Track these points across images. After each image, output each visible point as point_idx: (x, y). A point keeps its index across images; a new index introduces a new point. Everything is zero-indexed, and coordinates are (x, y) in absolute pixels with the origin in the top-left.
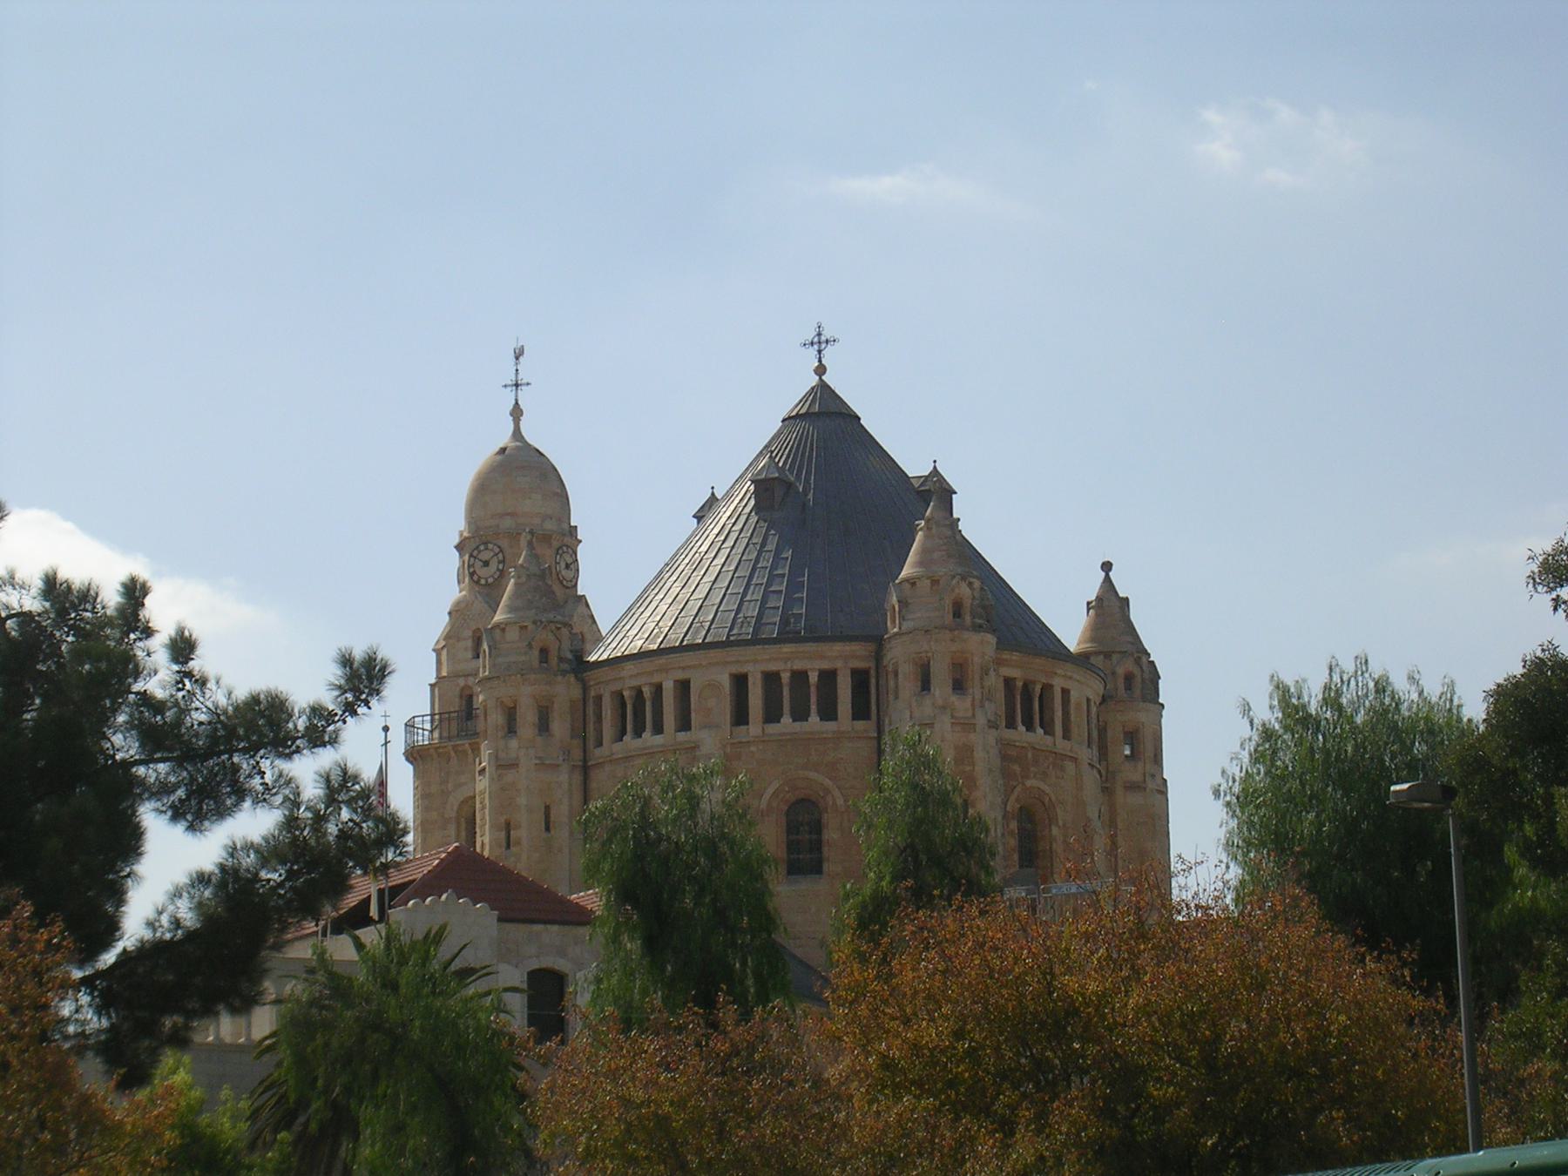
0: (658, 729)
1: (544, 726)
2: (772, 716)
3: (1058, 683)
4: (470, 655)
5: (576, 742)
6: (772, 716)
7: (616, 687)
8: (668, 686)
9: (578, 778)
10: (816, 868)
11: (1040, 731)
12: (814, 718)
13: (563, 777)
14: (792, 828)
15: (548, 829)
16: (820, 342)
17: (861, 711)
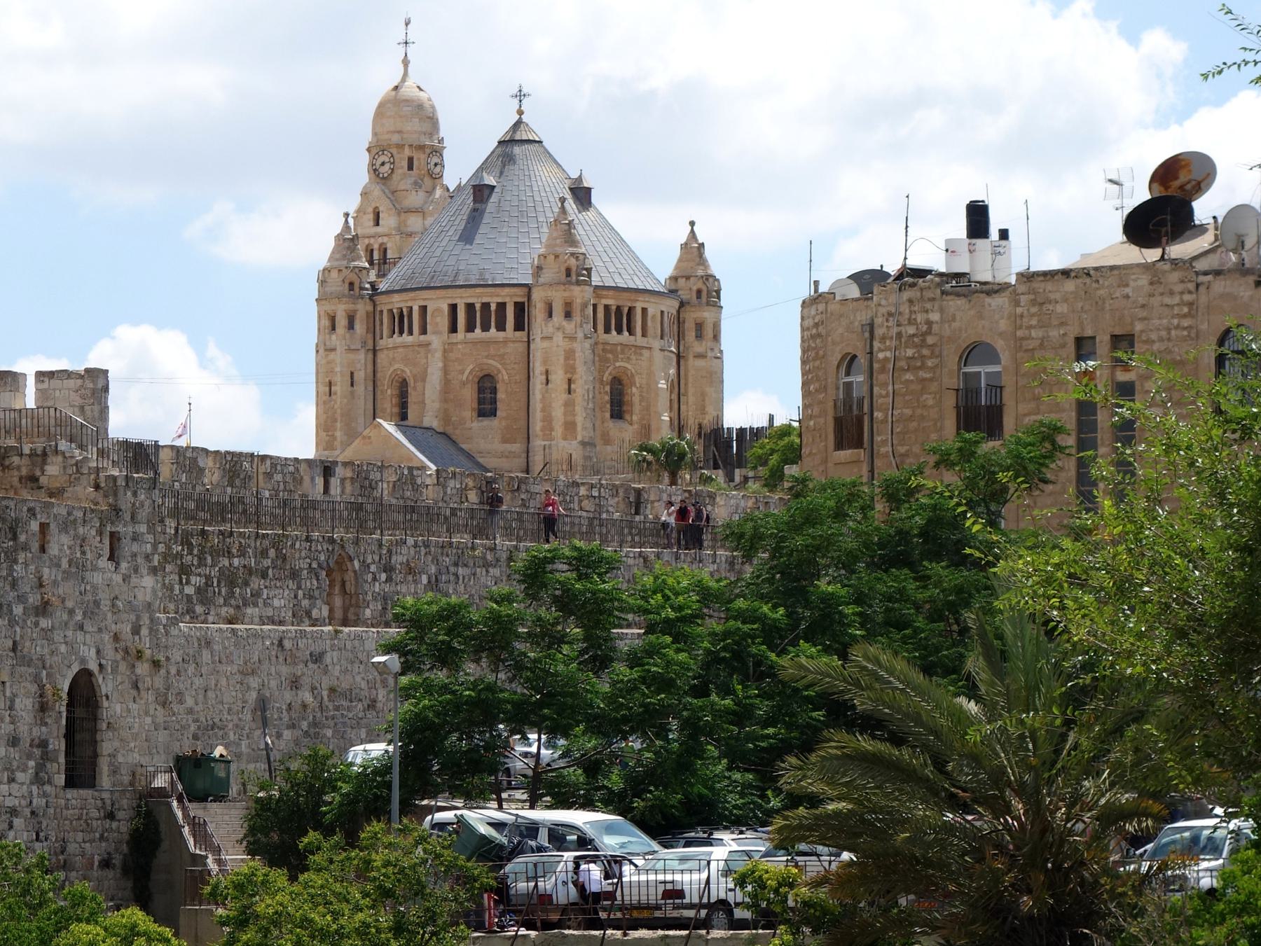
0: (411, 333)
1: (351, 326)
2: (470, 328)
3: (639, 306)
4: (372, 223)
5: (370, 336)
6: (470, 328)
7: (390, 307)
8: (416, 309)
9: (370, 356)
10: (493, 413)
11: (626, 333)
12: (493, 330)
13: (361, 356)
14: (481, 390)
15: (352, 385)
16: (520, 95)
17: (519, 326)
